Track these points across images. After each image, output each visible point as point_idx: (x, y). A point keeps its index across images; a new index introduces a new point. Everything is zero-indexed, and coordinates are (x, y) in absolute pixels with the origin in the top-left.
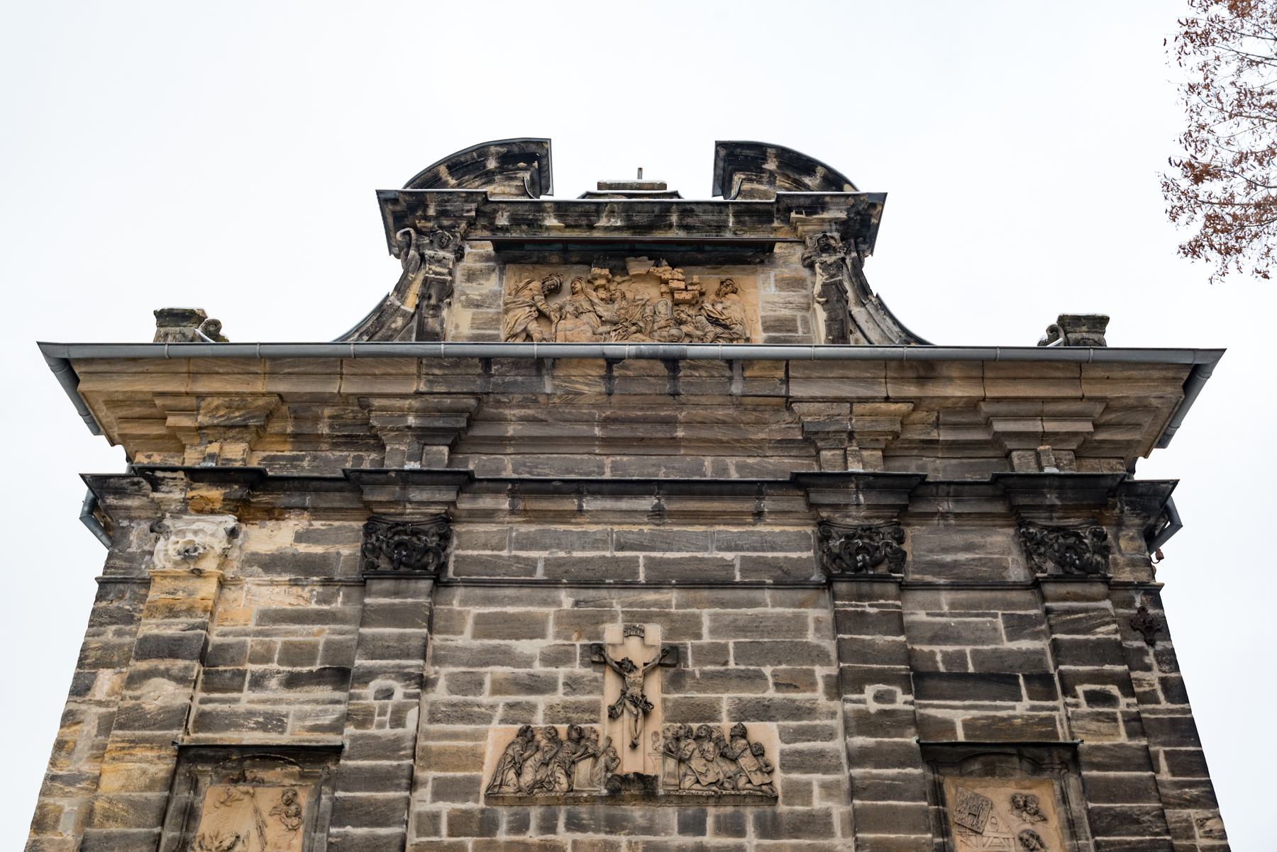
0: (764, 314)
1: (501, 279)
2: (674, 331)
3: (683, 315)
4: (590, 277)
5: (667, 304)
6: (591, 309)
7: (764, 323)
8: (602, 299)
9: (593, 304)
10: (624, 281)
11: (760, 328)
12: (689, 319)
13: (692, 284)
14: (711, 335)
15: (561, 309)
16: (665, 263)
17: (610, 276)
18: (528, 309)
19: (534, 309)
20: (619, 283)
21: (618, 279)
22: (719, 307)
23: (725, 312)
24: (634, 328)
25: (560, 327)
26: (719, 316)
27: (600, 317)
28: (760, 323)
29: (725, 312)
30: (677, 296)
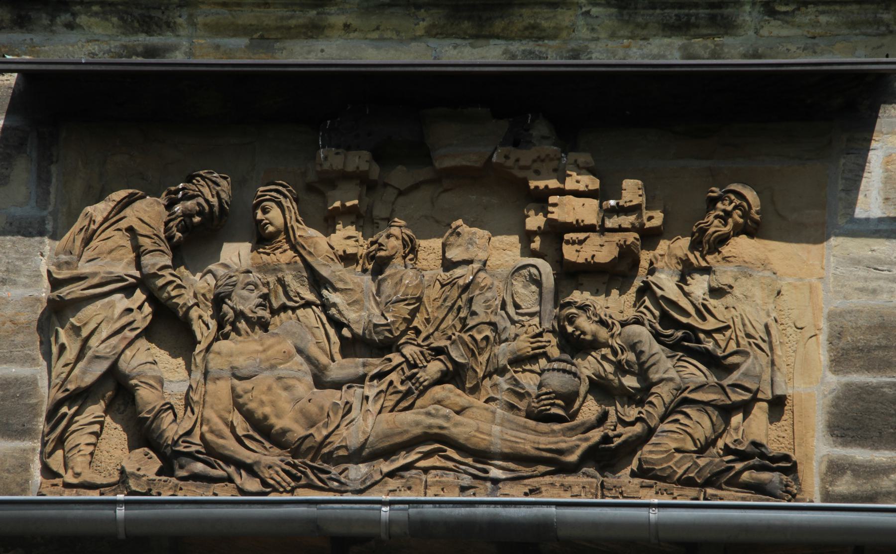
0: (838, 304)
1: (43, 179)
2: (556, 381)
3: (585, 324)
4: (311, 177)
5: (538, 283)
6: (310, 296)
7: (836, 336)
8: (348, 259)
9: (317, 282)
10: (415, 187)
11: (821, 355)
12: (603, 334)
13: (620, 210)
14: (663, 394)
15: (219, 301)
16: (541, 129)
17: (375, 172)
18: (120, 302)
19: (139, 296)
20: (401, 193)
21: (400, 176)
22: (699, 286)
23: (712, 303)
24: (435, 368)
25: (215, 363)
26: (695, 321)
27: (338, 325)
28: (823, 338)
29: (712, 303)
30: (570, 253)
